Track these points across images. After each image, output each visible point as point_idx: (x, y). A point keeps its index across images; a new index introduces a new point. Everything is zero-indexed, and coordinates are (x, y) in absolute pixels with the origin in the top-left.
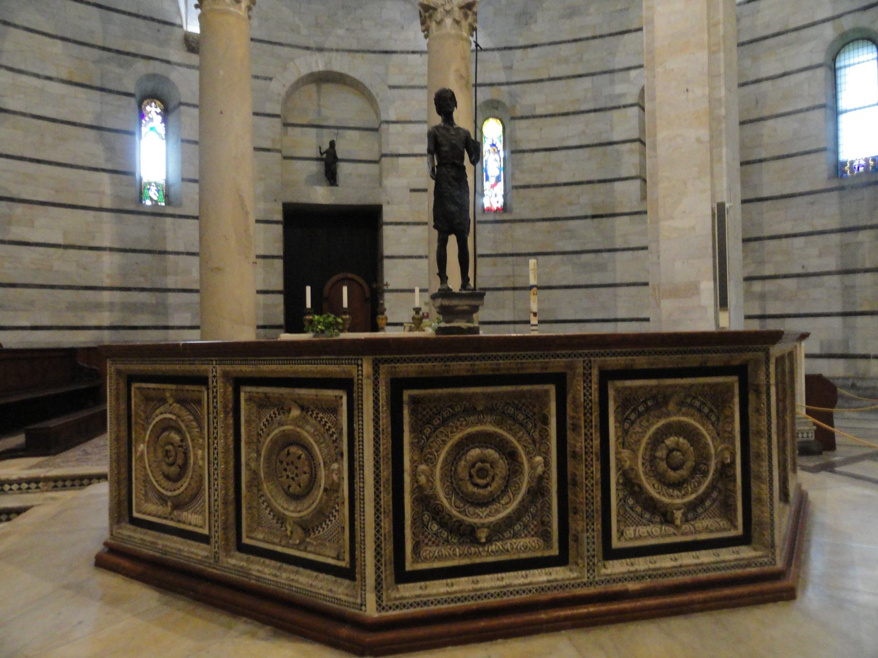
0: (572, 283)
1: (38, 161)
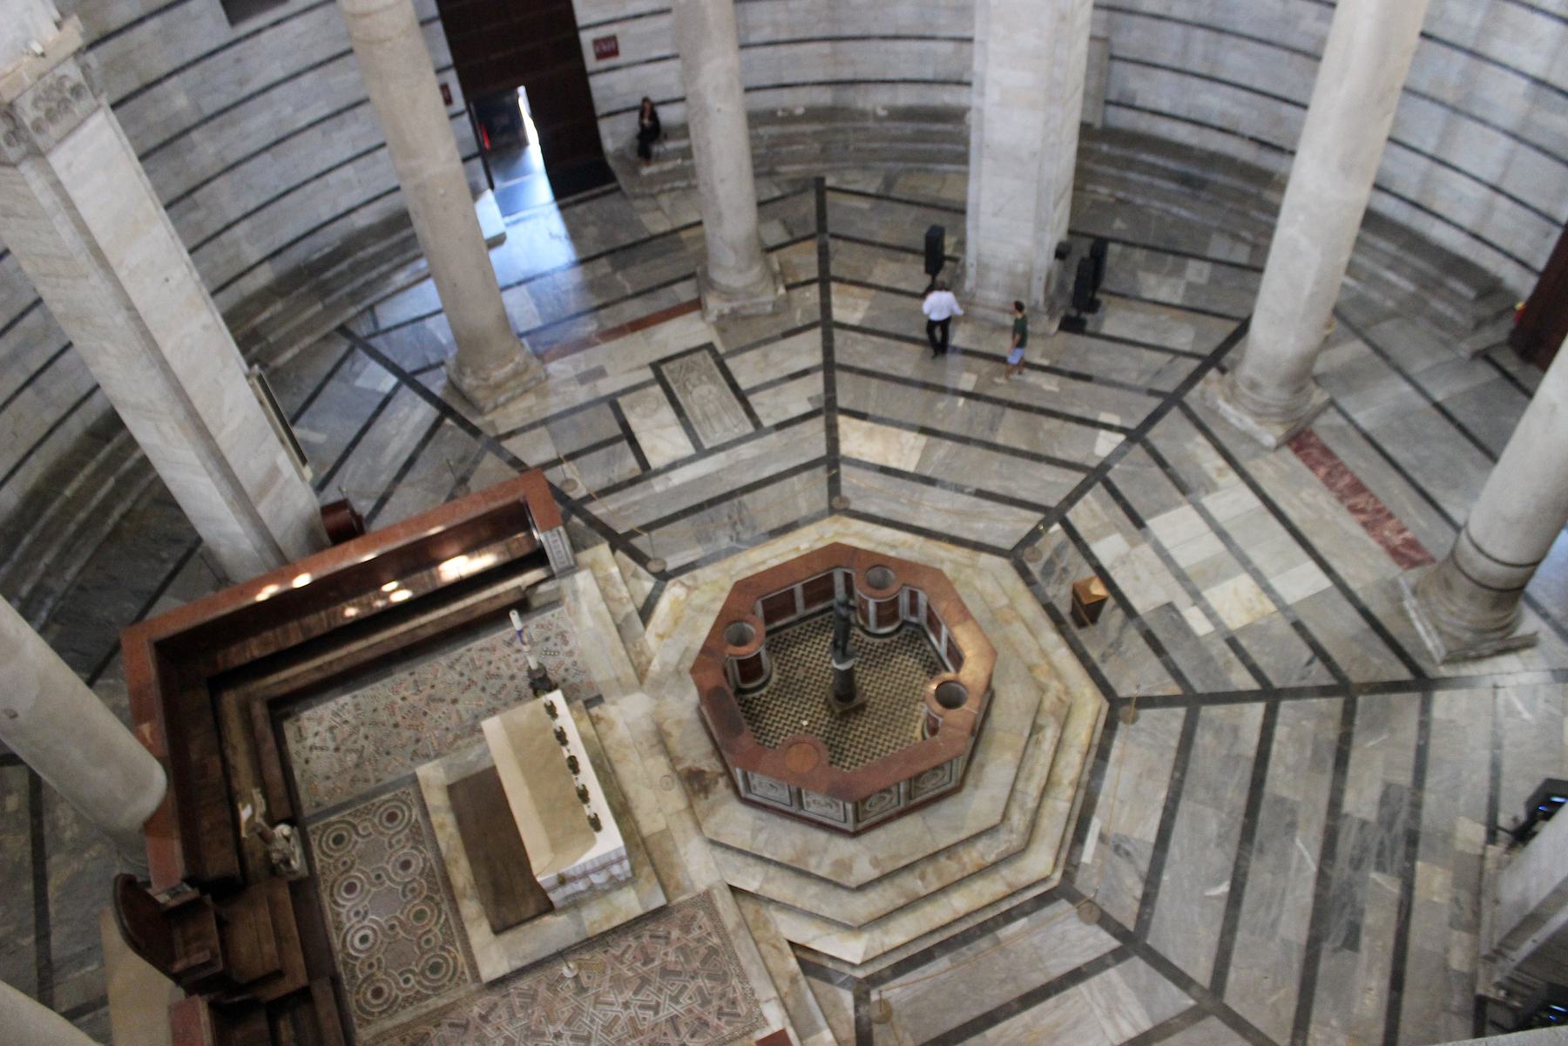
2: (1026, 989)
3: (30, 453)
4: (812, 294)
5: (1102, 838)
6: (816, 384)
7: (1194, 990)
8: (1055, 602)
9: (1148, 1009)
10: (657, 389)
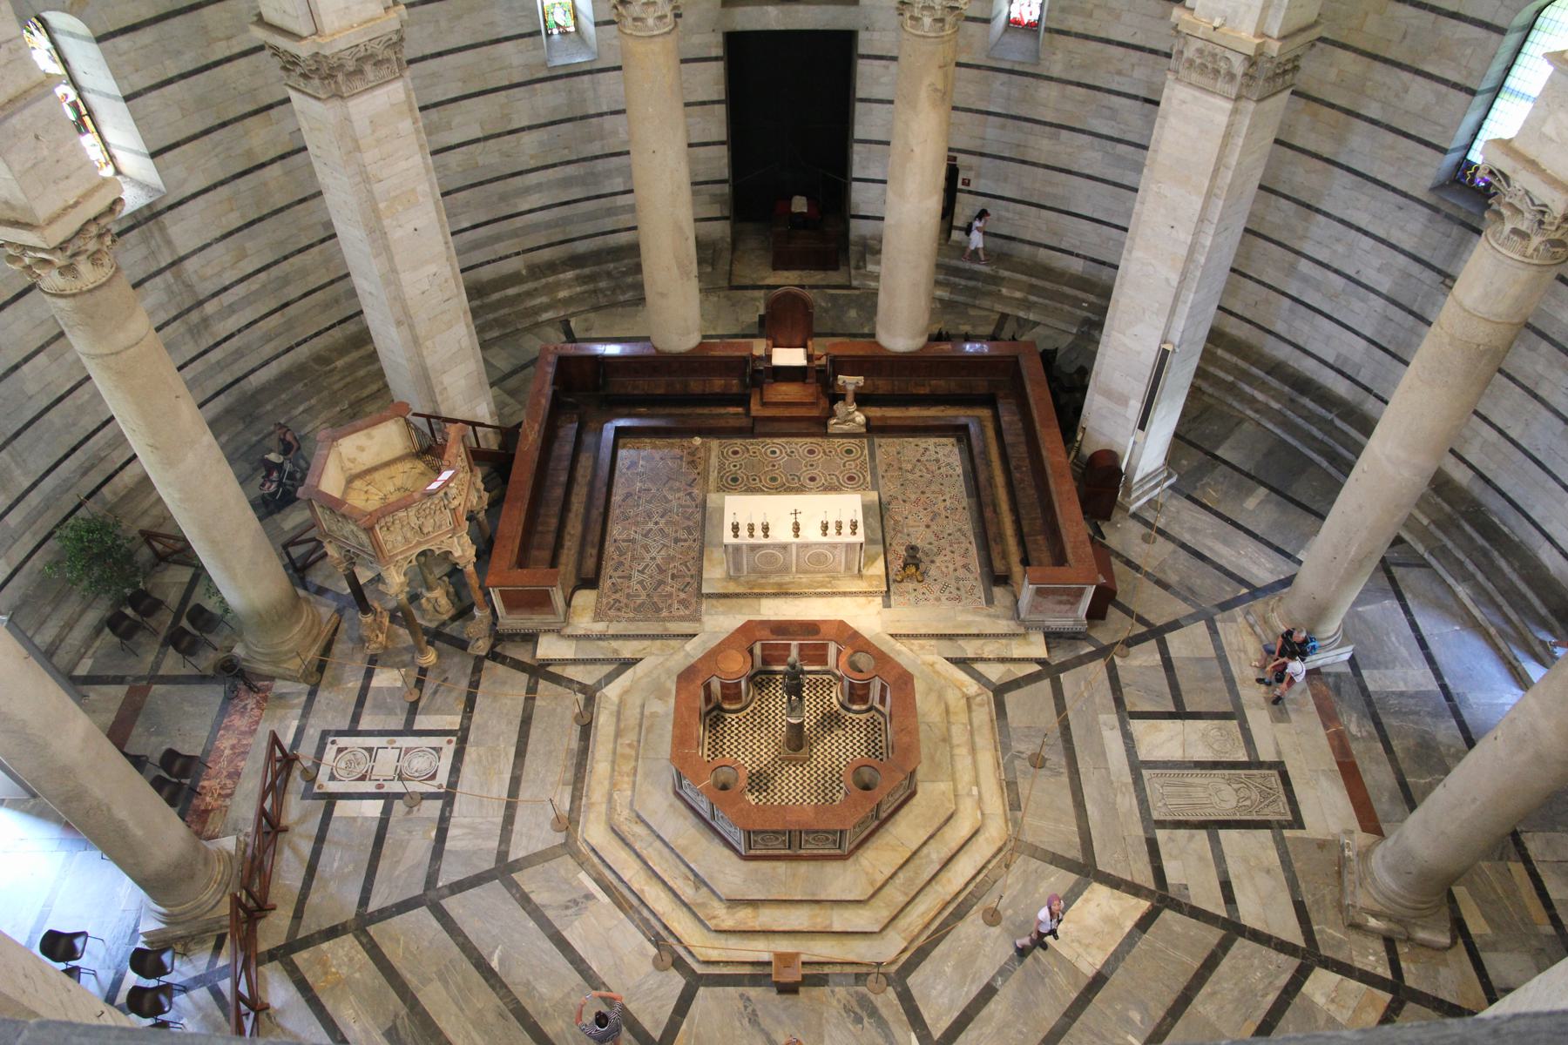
0: (1097, 175)
1: (440, 54)
2: (523, 785)
3: (1249, 322)
5: (589, 896)
7: (446, 891)
8: (827, 989)
9: (455, 853)
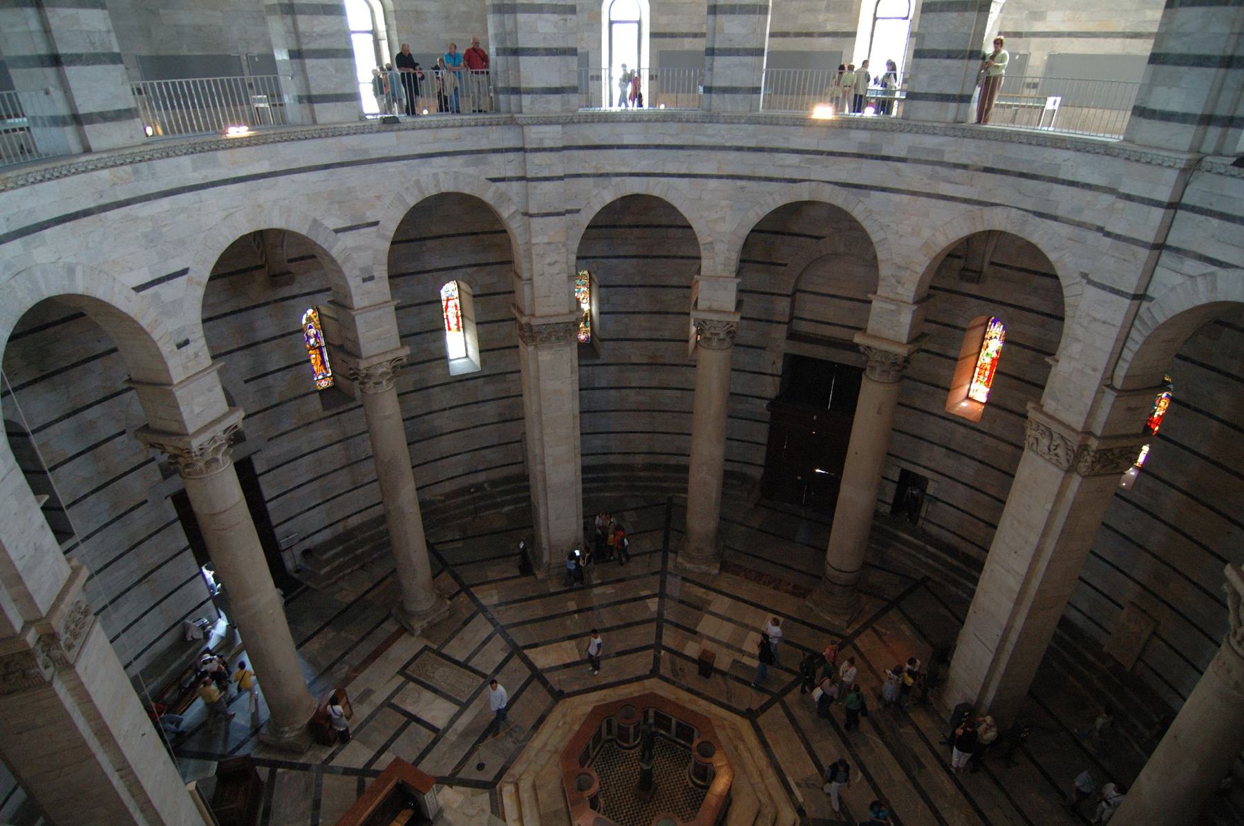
4: (463, 598)
5: (798, 784)
6: (499, 642)
10: (412, 684)
